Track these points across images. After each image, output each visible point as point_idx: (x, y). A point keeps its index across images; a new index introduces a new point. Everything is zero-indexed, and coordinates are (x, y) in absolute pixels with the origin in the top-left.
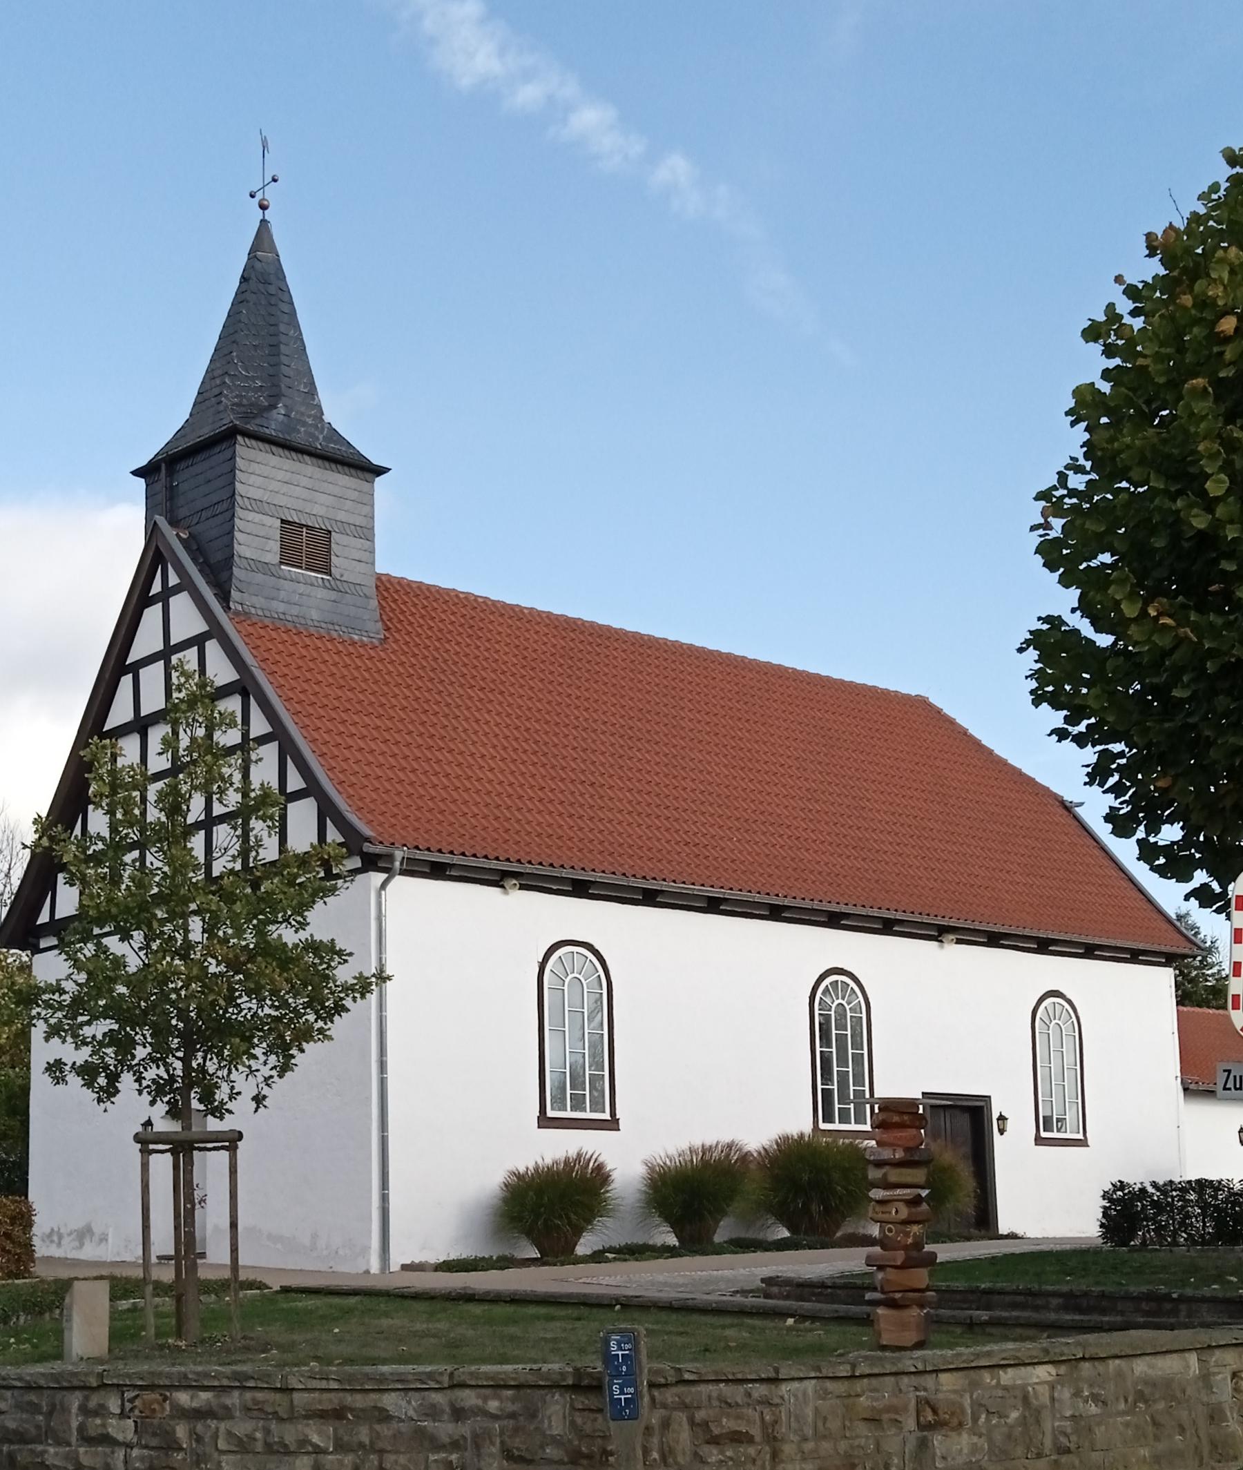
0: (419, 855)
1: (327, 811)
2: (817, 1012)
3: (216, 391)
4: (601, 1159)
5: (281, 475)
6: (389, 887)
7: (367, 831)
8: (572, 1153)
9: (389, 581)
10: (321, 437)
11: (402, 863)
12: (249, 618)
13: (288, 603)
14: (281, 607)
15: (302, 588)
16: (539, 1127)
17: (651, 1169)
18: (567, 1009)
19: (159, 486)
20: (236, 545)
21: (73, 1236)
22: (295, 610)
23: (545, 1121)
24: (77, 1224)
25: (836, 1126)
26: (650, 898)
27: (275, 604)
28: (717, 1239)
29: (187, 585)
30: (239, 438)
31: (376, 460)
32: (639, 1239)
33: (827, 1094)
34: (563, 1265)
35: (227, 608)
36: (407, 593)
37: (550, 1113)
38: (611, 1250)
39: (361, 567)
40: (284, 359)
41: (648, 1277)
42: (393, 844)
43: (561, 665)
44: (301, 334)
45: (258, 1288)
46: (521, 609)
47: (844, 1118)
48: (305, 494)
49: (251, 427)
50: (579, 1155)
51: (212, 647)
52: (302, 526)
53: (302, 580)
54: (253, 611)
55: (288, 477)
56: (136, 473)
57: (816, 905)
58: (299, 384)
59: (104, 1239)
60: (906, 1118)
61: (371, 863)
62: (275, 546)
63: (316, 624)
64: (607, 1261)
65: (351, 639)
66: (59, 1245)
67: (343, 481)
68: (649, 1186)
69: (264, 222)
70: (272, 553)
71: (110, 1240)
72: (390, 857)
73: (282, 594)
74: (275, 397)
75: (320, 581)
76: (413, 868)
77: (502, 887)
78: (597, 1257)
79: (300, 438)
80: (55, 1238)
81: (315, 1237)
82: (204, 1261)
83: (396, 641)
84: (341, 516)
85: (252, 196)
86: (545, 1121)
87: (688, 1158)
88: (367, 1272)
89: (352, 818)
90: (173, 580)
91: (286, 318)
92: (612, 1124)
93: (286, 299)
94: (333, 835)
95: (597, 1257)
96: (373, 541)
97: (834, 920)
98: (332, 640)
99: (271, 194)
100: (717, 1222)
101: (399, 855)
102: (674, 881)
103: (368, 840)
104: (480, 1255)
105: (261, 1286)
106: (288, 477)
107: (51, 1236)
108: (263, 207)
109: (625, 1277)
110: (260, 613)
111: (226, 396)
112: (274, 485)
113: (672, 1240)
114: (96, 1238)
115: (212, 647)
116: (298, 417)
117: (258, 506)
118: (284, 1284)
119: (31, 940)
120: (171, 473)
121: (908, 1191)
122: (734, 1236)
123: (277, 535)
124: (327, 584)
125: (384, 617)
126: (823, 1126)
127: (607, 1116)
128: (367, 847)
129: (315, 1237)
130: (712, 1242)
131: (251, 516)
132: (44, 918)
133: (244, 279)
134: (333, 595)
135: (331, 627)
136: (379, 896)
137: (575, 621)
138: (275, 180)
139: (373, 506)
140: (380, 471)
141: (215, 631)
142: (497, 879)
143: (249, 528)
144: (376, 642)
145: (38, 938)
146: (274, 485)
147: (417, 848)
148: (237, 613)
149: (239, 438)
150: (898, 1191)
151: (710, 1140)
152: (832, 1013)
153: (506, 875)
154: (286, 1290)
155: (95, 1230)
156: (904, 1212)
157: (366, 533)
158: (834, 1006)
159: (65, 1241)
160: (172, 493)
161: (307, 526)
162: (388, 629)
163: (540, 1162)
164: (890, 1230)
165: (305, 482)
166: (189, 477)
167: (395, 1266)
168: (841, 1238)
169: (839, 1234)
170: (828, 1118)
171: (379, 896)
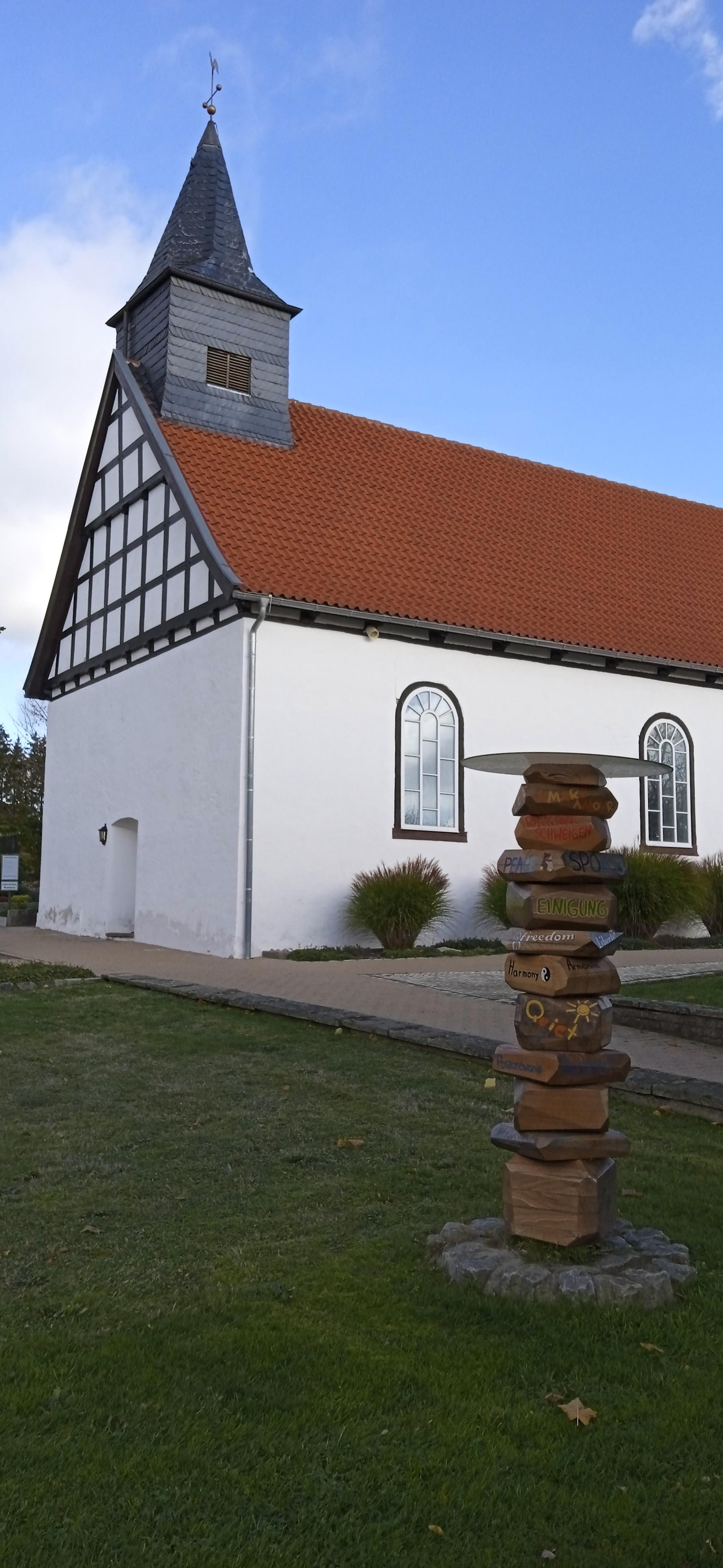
0: (282, 602)
3: (164, 252)
5: (209, 311)
7: (236, 580)
8: (413, 859)
10: (245, 283)
12: (177, 423)
13: (212, 413)
14: (206, 417)
15: (224, 402)
16: (394, 837)
19: (122, 333)
20: (168, 366)
22: (219, 419)
23: (399, 833)
24: (64, 907)
25: (662, 843)
26: (499, 649)
27: (200, 413)
30: (173, 279)
31: (290, 301)
33: (654, 817)
34: (396, 957)
36: (322, 417)
37: (404, 826)
39: (277, 389)
40: (217, 223)
42: (260, 592)
43: (567, 597)
44: (234, 205)
45: (79, 976)
46: (419, 435)
47: (668, 836)
48: (229, 327)
51: (146, 446)
52: (227, 353)
53: (225, 396)
54: (181, 418)
55: (215, 312)
56: (112, 323)
57: (645, 658)
58: (230, 242)
59: (77, 919)
60: (574, 795)
61: (247, 609)
62: (204, 369)
63: (235, 431)
65: (265, 444)
66: (54, 921)
67: (262, 316)
69: (211, 124)
70: (200, 373)
71: (81, 918)
72: (258, 603)
73: (207, 407)
74: (208, 251)
75: (241, 398)
76: (279, 615)
77: (366, 635)
78: (430, 952)
79: (227, 281)
80: (52, 915)
81: (200, 925)
82: (130, 940)
83: (304, 449)
84: (260, 346)
85: (205, 107)
86: (399, 833)
88: (231, 957)
90: (125, 399)
91: (223, 193)
92: (461, 836)
93: (224, 178)
95: (430, 952)
97: (662, 673)
98: (247, 444)
99: (216, 103)
101: (265, 601)
102: (519, 635)
103: (236, 587)
104: (330, 945)
105: (90, 973)
106: (215, 312)
107: (51, 914)
108: (211, 113)
110: (187, 420)
111: (171, 253)
112: (202, 318)
114: (73, 917)
115: (146, 446)
116: (227, 267)
117: (188, 335)
119: (47, 692)
120: (131, 319)
121: (568, 935)
123: (205, 359)
124: (246, 400)
125: (298, 431)
126: (649, 843)
128: (237, 594)
129: (200, 925)
131: (182, 342)
132: (52, 675)
133: (193, 165)
135: (248, 434)
136: (250, 637)
137: (464, 446)
138: (218, 89)
139: (287, 339)
140: (294, 312)
141: (148, 435)
143: (180, 352)
144: (286, 447)
146: (202, 318)
147: (282, 596)
148: (167, 419)
149: (173, 279)
150: (554, 936)
153: (369, 623)
154: (106, 979)
156: (561, 979)
157: (281, 360)
158: (661, 745)
159: (58, 917)
161: (232, 355)
162: (299, 440)
164: (535, 1010)
166: (142, 317)
167: (256, 952)
170: (653, 837)
171: (250, 637)
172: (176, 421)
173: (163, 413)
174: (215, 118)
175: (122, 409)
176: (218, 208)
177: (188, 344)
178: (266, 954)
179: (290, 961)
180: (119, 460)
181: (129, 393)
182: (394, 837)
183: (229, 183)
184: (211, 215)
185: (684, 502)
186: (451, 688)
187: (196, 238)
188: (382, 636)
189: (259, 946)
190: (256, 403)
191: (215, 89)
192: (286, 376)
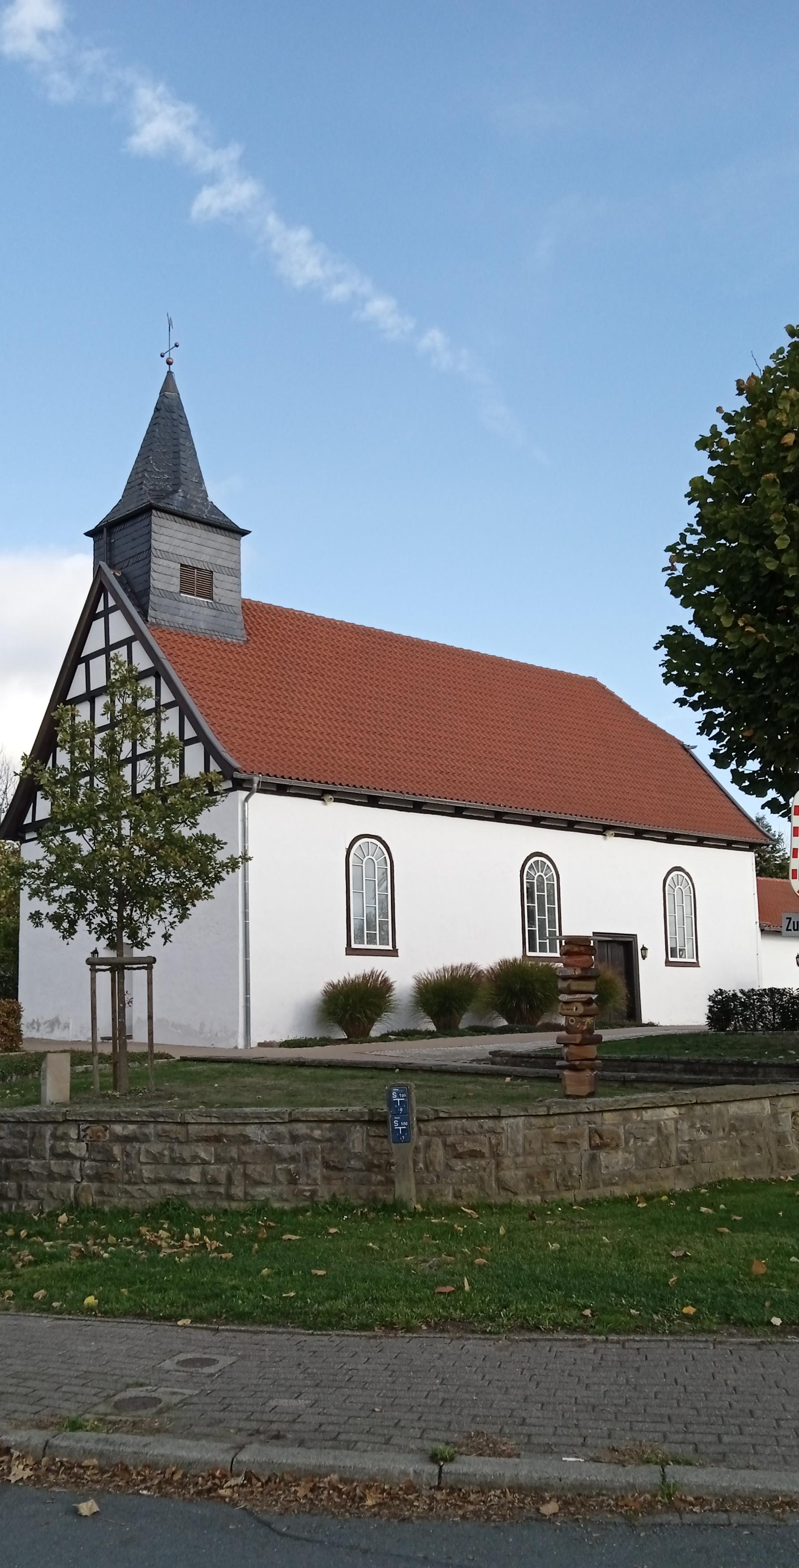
0: (269, 780)
1: (210, 751)
2: (525, 881)
3: (139, 481)
4: (386, 975)
5: (180, 535)
6: (250, 800)
7: (236, 764)
8: (368, 971)
9: (250, 604)
11: (258, 785)
14: (181, 620)
15: (194, 608)
16: (347, 954)
17: (419, 981)
18: (364, 878)
20: (152, 581)
21: (47, 1024)
22: (190, 622)
24: (50, 1016)
25: (538, 954)
26: (418, 807)
28: (461, 1026)
29: (120, 606)
30: (154, 511)
31: (242, 526)
32: (411, 1026)
33: (532, 934)
34: (362, 1043)
35: (146, 621)
36: (262, 611)
37: (354, 946)
38: (393, 1033)
41: (417, 1051)
43: (360, 658)
46: (335, 621)
47: (543, 949)
48: (196, 547)
49: (162, 505)
50: (372, 973)
51: (137, 646)
52: (194, 568)
54: (163, 623)
55: (185, 536)
56: (88, 534)
57: (524, 812)
59: (67, 1026)
60: (582, 948)
61: (239, 785)
62: (177, 581)
64: (391, 1040)
66: (38, 1030)
67: (220, 539)
68: (417, 993)
69: (170, 373)
70: (175, 585)
71: (71, 1027)
72: (251, 781)
73: (182, 612)
74: (177, 485)
76: (266, 789)
77: (323, 800)
78: (384, 1038)
79: (193, 511)
80: (36, 1026)
81: (202, 1025)
83: (255, 642)
84: (219, 562)
85: (162, 356)
87: (442, 974)
88: (236, 1048)
89: (227, 756)
90: (111, 603)
91: (184, 434)
92: (394, 953)
93: (184, 422)
94: (214, 767)
95: (384, 1038)
96: (239, 578)
97: (536, 822)
98: (213, 641)
99: (174, 354)
100: (461, 1015)
101: (256, 779)
103: (236, 770)
104: (309, 1037)
105: (168, 1057)
106: (185, 536)
107: (33, 1024)
108: (169, 363)
109: (402, 1051)
110: (167, 624)
111: (145, 485)
113: (432, 1027)
115: (137, 646)
117: (166, 556)
118: (182, 1055)
119: (20, 834)
120: (110, 534)
121: (583, 996)
122: (472, 1024)
123: (178, 574)
125: (247, 627)
126: (529, 954)
127: (390, 947)
129: (202, 1025)
130: (458, 1029)
131: (162, 562)
132: (28, 820)
133: (157, 409)
134: (214, 613)
136: (244, 806)
137: (370, 629)
138: (176, 346)
139: (239, 555)
140: (244, 533)
141: (138, 635)
142: (320, 795)
143: (160, 569)
145: (25, 833)
147: (268, 775)
148: (152, 624)
149: (154, 511)
150: (577, 996)
151: (456, 963)
152: (535, 881)
153: (325, 792)
154: (184, 1059)
155: (61, 1020)
156: (581, 1009)
157: (235, 573)
160: (110, 547)
161: (197, 568)
162: (249, 634)
163: (347, 977)
164: (572, 1021)
165: (196, 539)
166: (121, 536)
168: (541, 1026)
169: (539, 1023)
170: (532, 949)
171: (244, 806)
172: (159, 625)
173: (149, 619)
174: (173, 368)
175: (107, 611)
176: (182, 447)
177: (166, 563)
178: (260, 1045)
179: (283, 1049)
180: (106, 650)
181: (116, 597)
182: (347, 954)
183: (188, 425)
184: (177, 454)
185: (541, 669)
186: (384, 838)
187: (167, 473)
188: (336, 800)
189: (255, 1040)
190: (217, 607)
191: (172, 345)
192: (239, 585)
